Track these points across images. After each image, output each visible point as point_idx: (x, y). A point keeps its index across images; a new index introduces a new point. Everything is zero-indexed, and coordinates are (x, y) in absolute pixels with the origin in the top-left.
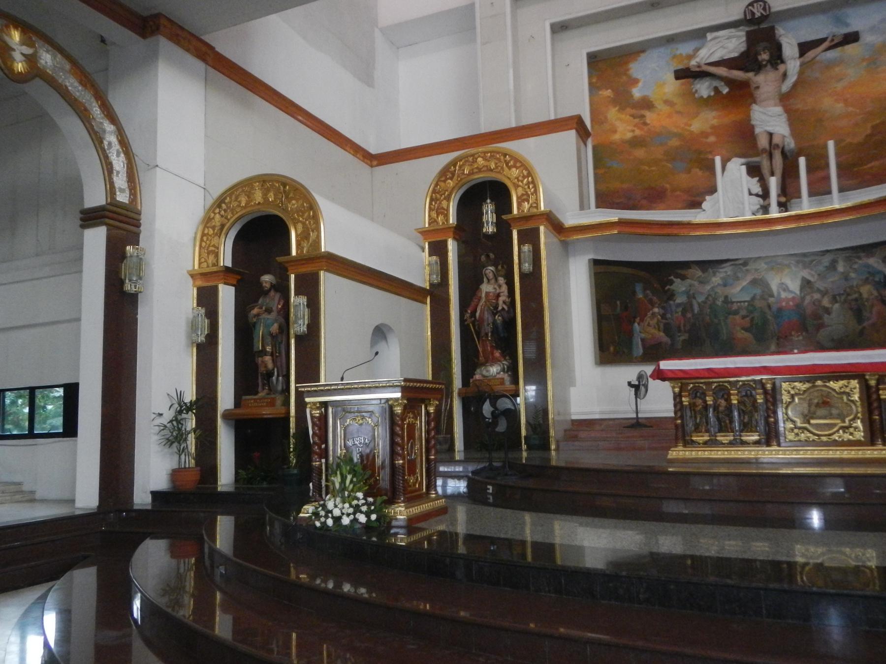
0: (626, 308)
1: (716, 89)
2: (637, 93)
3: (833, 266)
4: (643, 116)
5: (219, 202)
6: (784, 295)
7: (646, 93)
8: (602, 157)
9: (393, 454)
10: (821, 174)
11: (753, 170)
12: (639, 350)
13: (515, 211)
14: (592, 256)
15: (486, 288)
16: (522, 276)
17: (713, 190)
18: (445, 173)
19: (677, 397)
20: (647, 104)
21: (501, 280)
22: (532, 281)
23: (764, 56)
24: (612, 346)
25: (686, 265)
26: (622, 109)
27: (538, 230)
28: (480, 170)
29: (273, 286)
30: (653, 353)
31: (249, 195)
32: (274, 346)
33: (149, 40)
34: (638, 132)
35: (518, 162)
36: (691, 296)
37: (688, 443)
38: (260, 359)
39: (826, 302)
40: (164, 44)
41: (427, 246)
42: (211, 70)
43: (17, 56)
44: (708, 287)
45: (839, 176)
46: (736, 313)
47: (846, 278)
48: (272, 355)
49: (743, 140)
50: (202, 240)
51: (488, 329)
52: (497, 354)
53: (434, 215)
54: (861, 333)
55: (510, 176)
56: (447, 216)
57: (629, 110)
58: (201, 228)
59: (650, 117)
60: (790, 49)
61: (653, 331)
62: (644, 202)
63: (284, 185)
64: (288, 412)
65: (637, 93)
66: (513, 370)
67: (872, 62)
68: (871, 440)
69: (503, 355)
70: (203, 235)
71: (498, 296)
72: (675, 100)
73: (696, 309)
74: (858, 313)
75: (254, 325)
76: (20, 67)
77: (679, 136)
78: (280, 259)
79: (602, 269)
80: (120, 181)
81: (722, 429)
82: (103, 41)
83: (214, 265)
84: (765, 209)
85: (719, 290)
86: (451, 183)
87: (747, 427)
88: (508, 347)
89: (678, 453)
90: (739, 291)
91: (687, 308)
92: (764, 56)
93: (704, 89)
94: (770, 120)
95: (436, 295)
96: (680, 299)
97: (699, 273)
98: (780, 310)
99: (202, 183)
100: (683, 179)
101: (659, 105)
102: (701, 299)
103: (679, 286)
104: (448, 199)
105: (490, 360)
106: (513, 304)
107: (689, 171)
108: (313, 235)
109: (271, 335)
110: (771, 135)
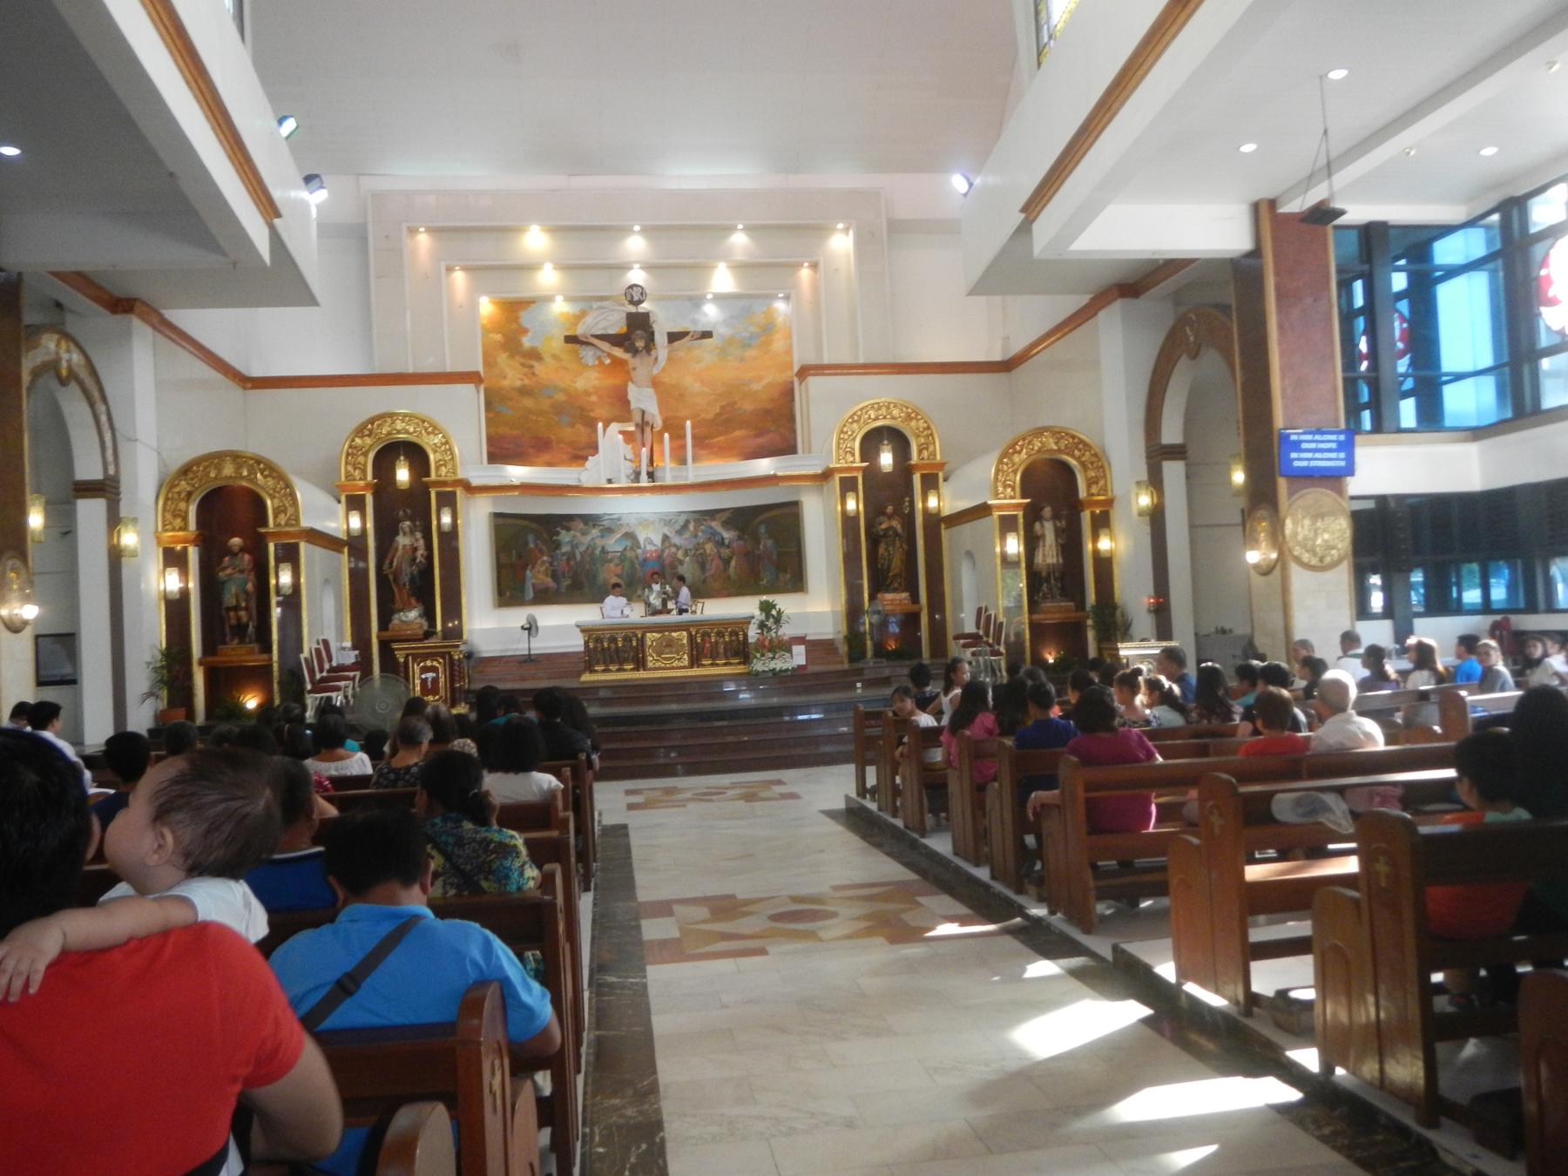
0: (520, 556)
1: (599, 358)
2: (527, 342)
3: (685, 526)
4: (532, 367)
5: (185, 471)
6: (649, 547)
7: (537, 344)
8: (492, 402)
9: (452, 682)
10: (679, 442)
11: (628, 437)
12: (530, 594)
13: (433, 476)
14: (492, 510)
15: (403, 541)
16: (441, 534)
17: (594, 448)
18: (360, 431)
19: (586, 643)
20: (535, 355)
21: (419, 535)
22: (450, 538)
23: (640, 344)
24: (509, 591)
25: (570, 518)
26: (512, 356)
27: (454, 494)
28: (399, 432)
29: (243, 550)
30: (545, 597)
31: (219, 469)
32: (247, 601)
33: (119, 317)
34: (527, 382)
35: (436, 429)
36: (574, 546)
37: (592, 671)
38: (232, 614)
39: (680, 555)
40: (136, 323)
41: (343, 499)
42: (159, 337)
43: (64, 364)
44: (588, 538)
45: (694, 446)
46: (610, 561)
47: (696, 536)
48: (246, 609)
49: (621, 407)
50: (165, 504)
51: (406, 579)
52: (413, 601)
53: (350, 468)
54: (704, 581)
55: (429, 442)
56: (364, 471)
57: (519, 359)
58: (164, 491)
59: (539, 368)
60: (661, 339)
61: (542, 576)
62: (531, 450)
63: (258, 462)
64: (271, 659)
65: (527, 342)
66: (429, 614)
67: (723, 351)
68: (691, 666)
69: (418, 601)
70: (167, 499)
71: (415, 549)
72: (563, 356)
73: (578, 556)
74: (703, 566)
75: (223, 583)
76: (64, 372)
77: (566, 391)
78: (263, 530)
79: (501, 521)
80: (110, 458)
81: (612, 662)
82: (59, 305)
83: (181, 529)
84: (637, 475)
85: (599, 542)
86: (368, 441)
87: (625, 661)
88: (422, 592)
89: (586, 677)
90: (614, 544)
91: (571, 556)
92: (640, 344)
93: (588, 355)
94: (643, 399)
95: (355, 545)
96: (565, 549)
97: (581, 526)
98: (645, 560)
99: (154, 444)
100: (567, 433)
101: (548, 359)
102: (582, 549)
103: (565, 537)
104: (365, 454)
105: (407, 607)
106: (430, 558)
107: (572, 426)
108: (290, 511)
109: (246, 593)
110: (643, 412)
